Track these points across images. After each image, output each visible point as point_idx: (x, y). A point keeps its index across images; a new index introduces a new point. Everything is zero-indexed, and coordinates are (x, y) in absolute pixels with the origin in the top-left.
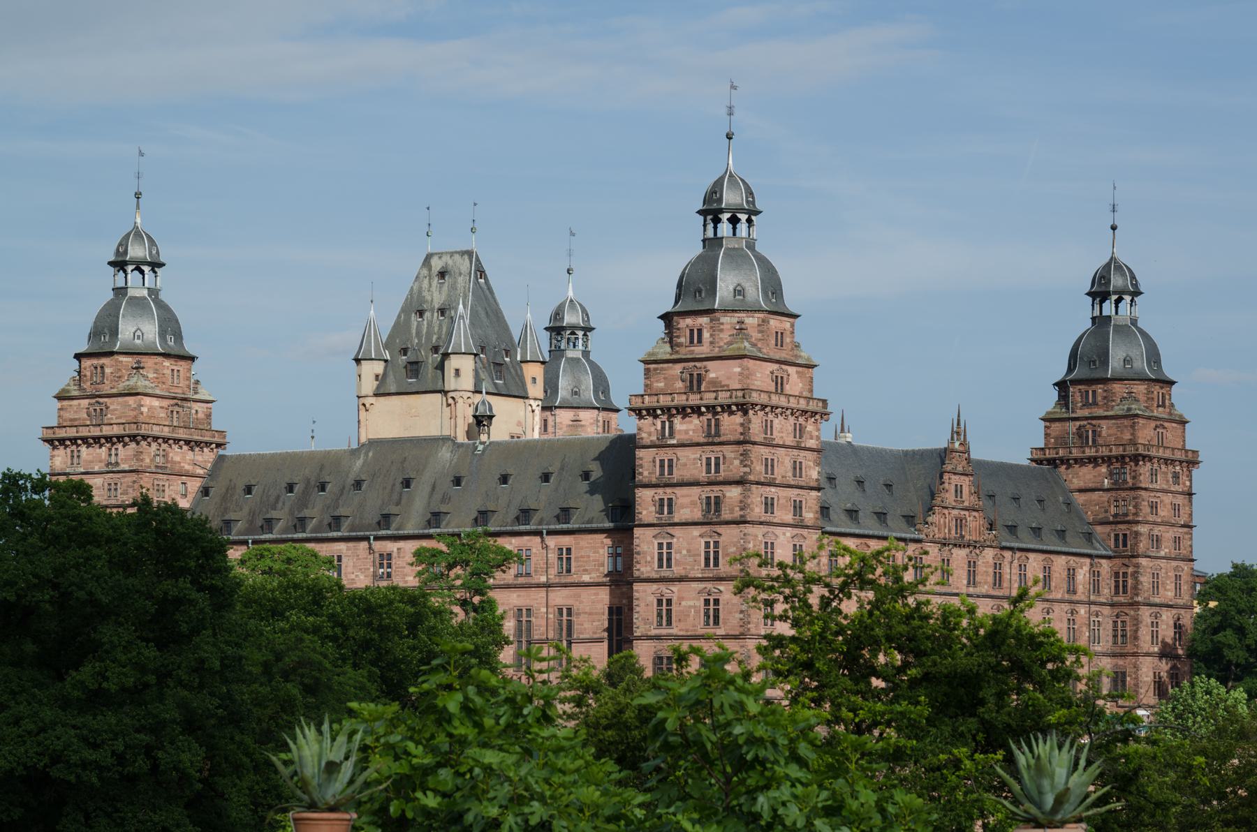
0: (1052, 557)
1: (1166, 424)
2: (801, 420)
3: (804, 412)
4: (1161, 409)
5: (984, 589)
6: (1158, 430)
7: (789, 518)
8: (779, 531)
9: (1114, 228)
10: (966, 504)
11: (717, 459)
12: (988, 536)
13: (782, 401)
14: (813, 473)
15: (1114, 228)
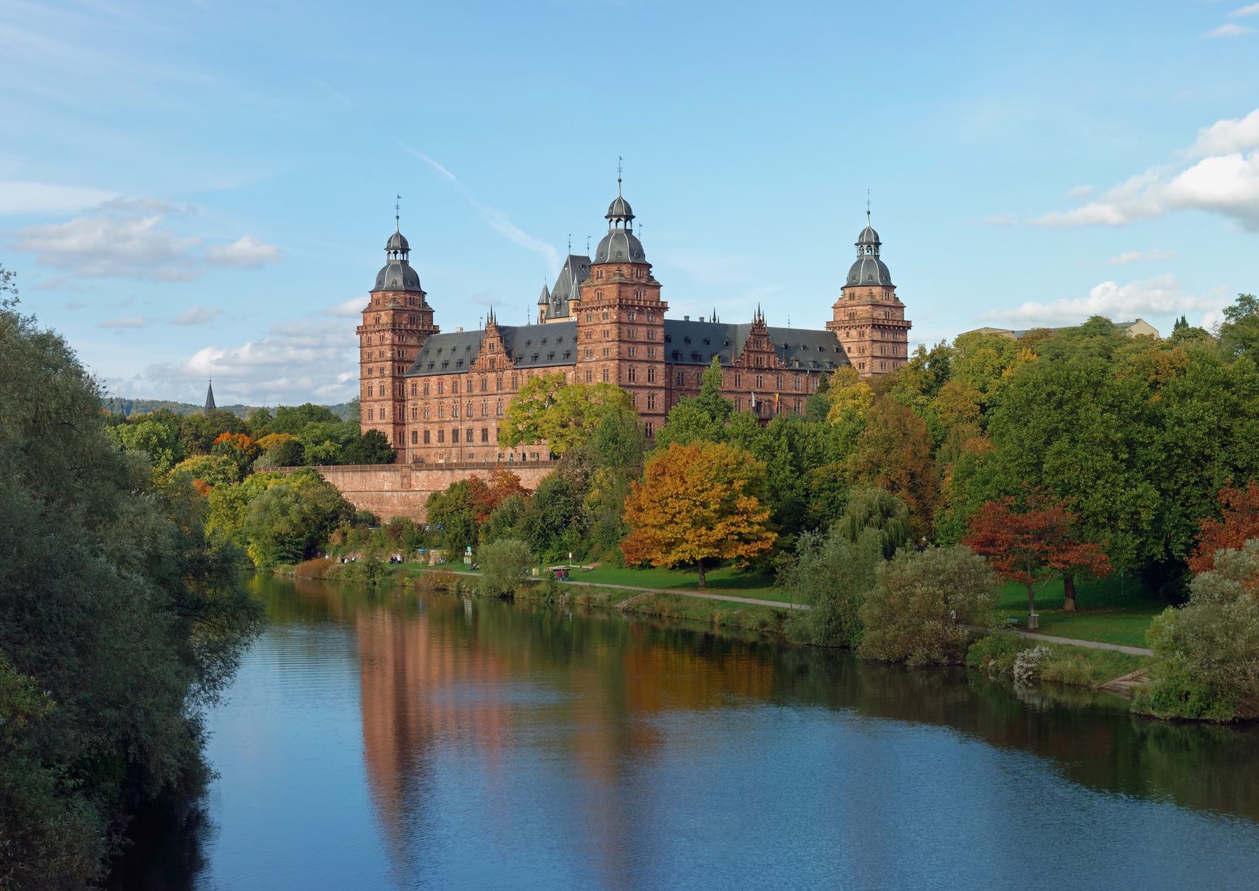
0: (549, 369)
1: (604, 287)
2: (382, 333)
3: (384, 330)
4: (599, 280)
5: (507, 390)
6: (597, 292)
7: (378, 375)
8: (373, 381)
9: (620, 181)
10: (496, 351)
11: (403, 352)
12: (509, 364)
13: (381, 328)
14: (389, 355)
15: (620, 181)
